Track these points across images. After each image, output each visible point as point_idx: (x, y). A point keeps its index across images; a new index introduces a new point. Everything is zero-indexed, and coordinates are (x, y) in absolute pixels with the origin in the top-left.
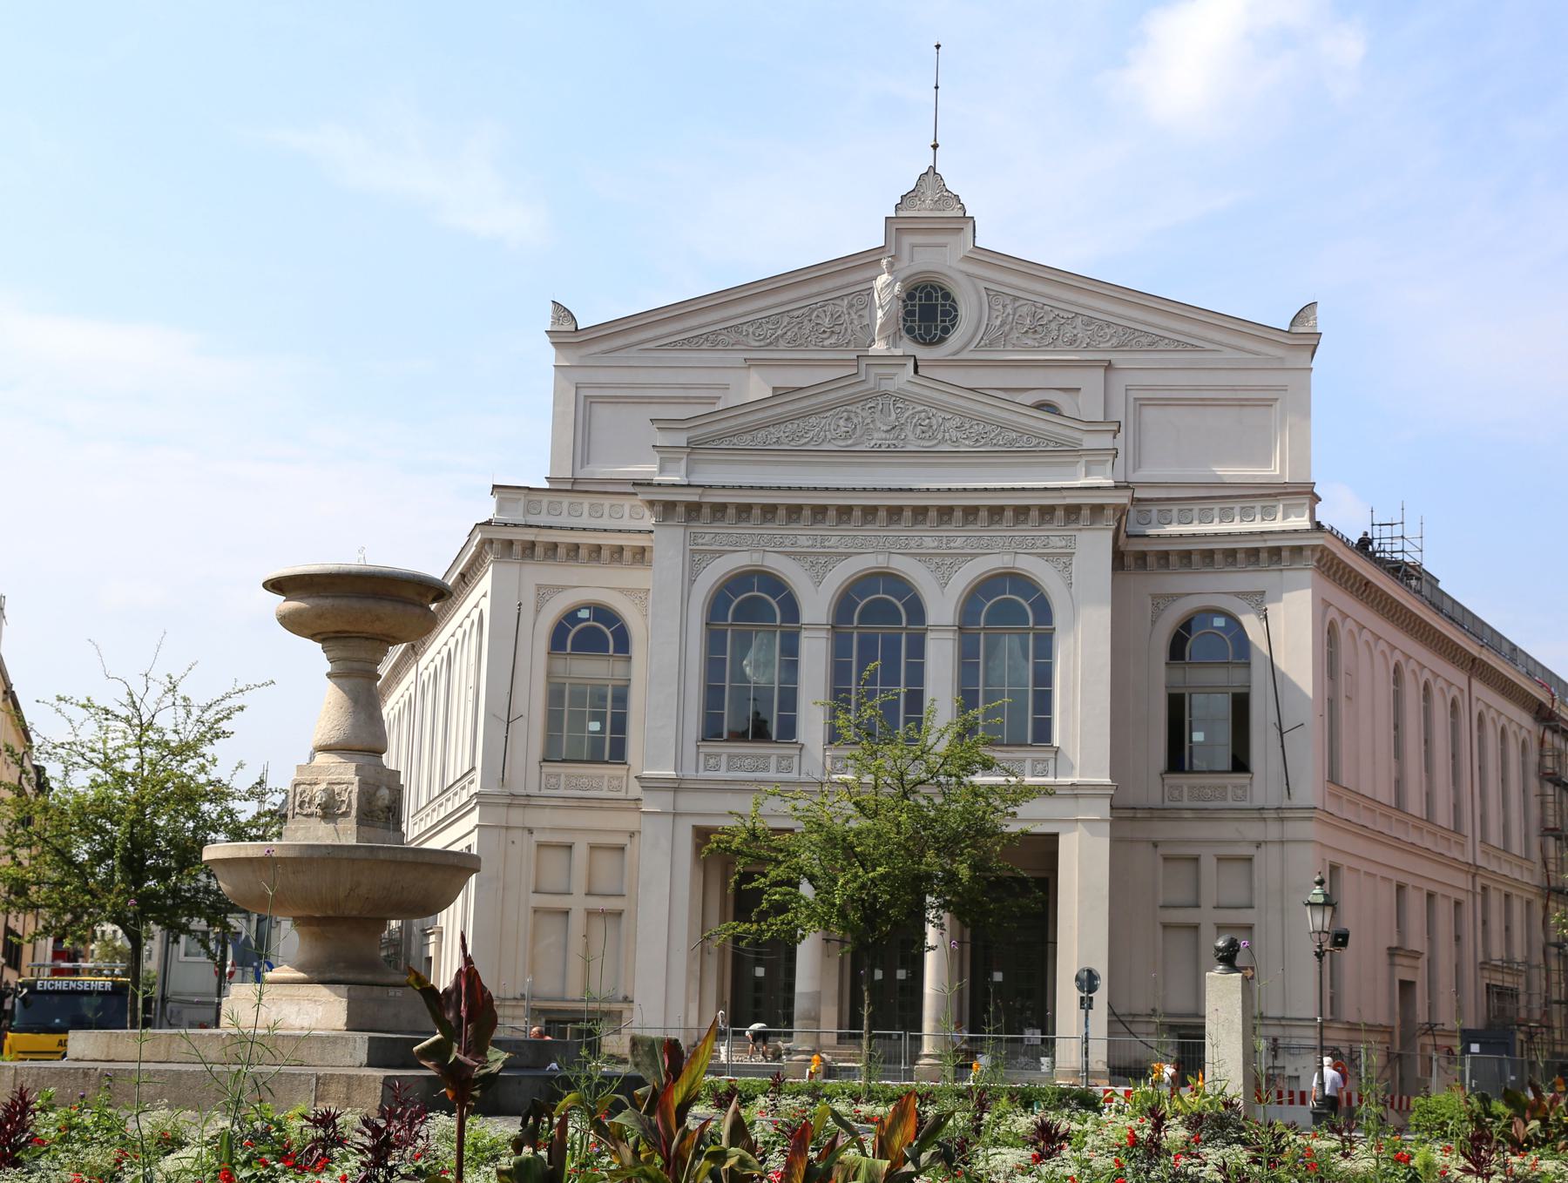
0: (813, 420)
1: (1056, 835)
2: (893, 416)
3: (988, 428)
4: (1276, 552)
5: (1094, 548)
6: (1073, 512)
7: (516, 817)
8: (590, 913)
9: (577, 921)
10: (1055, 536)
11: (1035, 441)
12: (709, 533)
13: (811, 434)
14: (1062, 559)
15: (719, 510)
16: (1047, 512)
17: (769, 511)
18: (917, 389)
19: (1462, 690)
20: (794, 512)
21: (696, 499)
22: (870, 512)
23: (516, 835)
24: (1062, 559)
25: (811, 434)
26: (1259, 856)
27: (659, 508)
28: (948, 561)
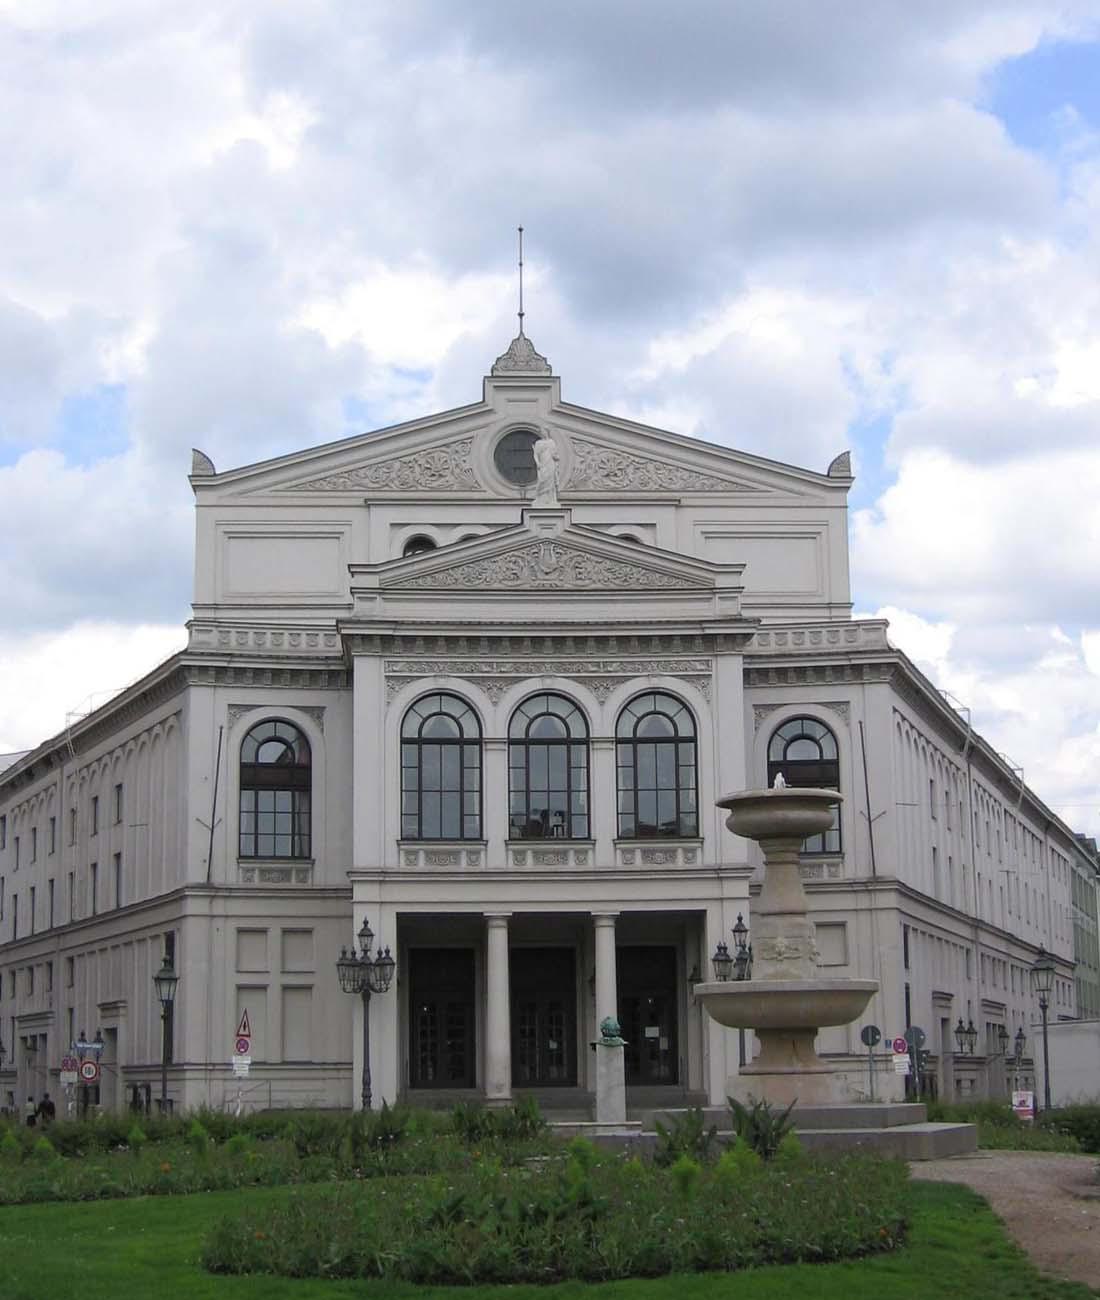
0: (485, 564)
1: (705, 911)
3: (635, 570)
4: (858, 669)
5: (729, 669)
7: (219, 907)
8: (286, 988)
9: (274, 993)
10: (694, 661)
11: (674, 581)
12: (402, 663)
14: (700, 679)
17: (452, 641)
19: (964, 774)
20: (473, 641)
23: (219, 922)
24: (700, 679)
26: (852, 922)
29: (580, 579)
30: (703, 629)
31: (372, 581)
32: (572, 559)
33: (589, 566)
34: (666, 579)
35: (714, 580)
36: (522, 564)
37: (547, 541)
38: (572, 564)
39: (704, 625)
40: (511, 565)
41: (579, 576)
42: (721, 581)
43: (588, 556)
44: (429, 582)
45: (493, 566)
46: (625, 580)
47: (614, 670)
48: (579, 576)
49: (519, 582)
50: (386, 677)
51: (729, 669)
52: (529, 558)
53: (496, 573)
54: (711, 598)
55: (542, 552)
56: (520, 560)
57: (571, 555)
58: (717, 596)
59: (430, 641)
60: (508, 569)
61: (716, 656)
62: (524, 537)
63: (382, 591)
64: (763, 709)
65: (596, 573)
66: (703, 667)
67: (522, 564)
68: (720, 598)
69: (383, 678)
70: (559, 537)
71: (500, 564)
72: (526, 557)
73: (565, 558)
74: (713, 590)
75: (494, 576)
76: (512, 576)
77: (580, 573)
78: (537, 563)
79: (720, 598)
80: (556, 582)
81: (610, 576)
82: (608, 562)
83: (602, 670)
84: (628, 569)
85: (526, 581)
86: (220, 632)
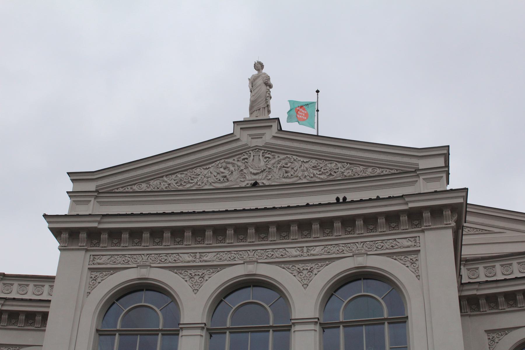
0: (198, 171)
2: (262, 163)
3: (339, 165)
6: (415, 216)
13: (195, 180)
14: (410, 255)
15: (115, 235)
16: (392, 218)
17: (156, 234)
18: (279, 142)
20: (177, 233)
21: (95, 225)
22: (240, 230)
24: (410, 255)
25: (195, 180)
27: (65, 235)
28: (309, 266)
29: (287, 177)
30: (406, 203)
31: (91, 187)
32: (279, 162)
33: (297, 165)
34: (370, 170)
35: (418, 165)
36: (232, 168)
37: (257, 149)
38: (279, 166)
39: (407, 199)
40: (222, 170)
41: (286, 175)
42: (423, 164)
43: (295, 157)
44: (144, 187)
45: (206, 172)
46: (331, 174)
47: (318, 251)
48: (286, 175)
49: (227, 184)
50: (89, 268)
51: (436, 244)
52: (239, 164)
53: (208, 178)
54: (417, 181)
55: (252, 158)
56: (230, 166)
57: (277, 159)
58: (421, 177)
59: (136, 234)
60: (218, 173)
61: (423, 231)
62: (234, 145)
63: (98, 193)
64: (495, 334)
65: (304, 169)
66: (409, 243)
67: (232, 168)
68: (424, 179)
69: (86, 270)
70: (266, 143)
71: (211, 170)
72: (236, 162)
73: (273, 161)
74: (416, 172)
75: (205, 179)
76: (222, 179)
77: (286, 173)
78: (246, 168)
79: (424, 179)
80: (264, 181)
81: (315, 172)
82: (314, 161)
83: (305, 254)
84: (333, 165)
85: (235, 180)
86: (4, 284)
